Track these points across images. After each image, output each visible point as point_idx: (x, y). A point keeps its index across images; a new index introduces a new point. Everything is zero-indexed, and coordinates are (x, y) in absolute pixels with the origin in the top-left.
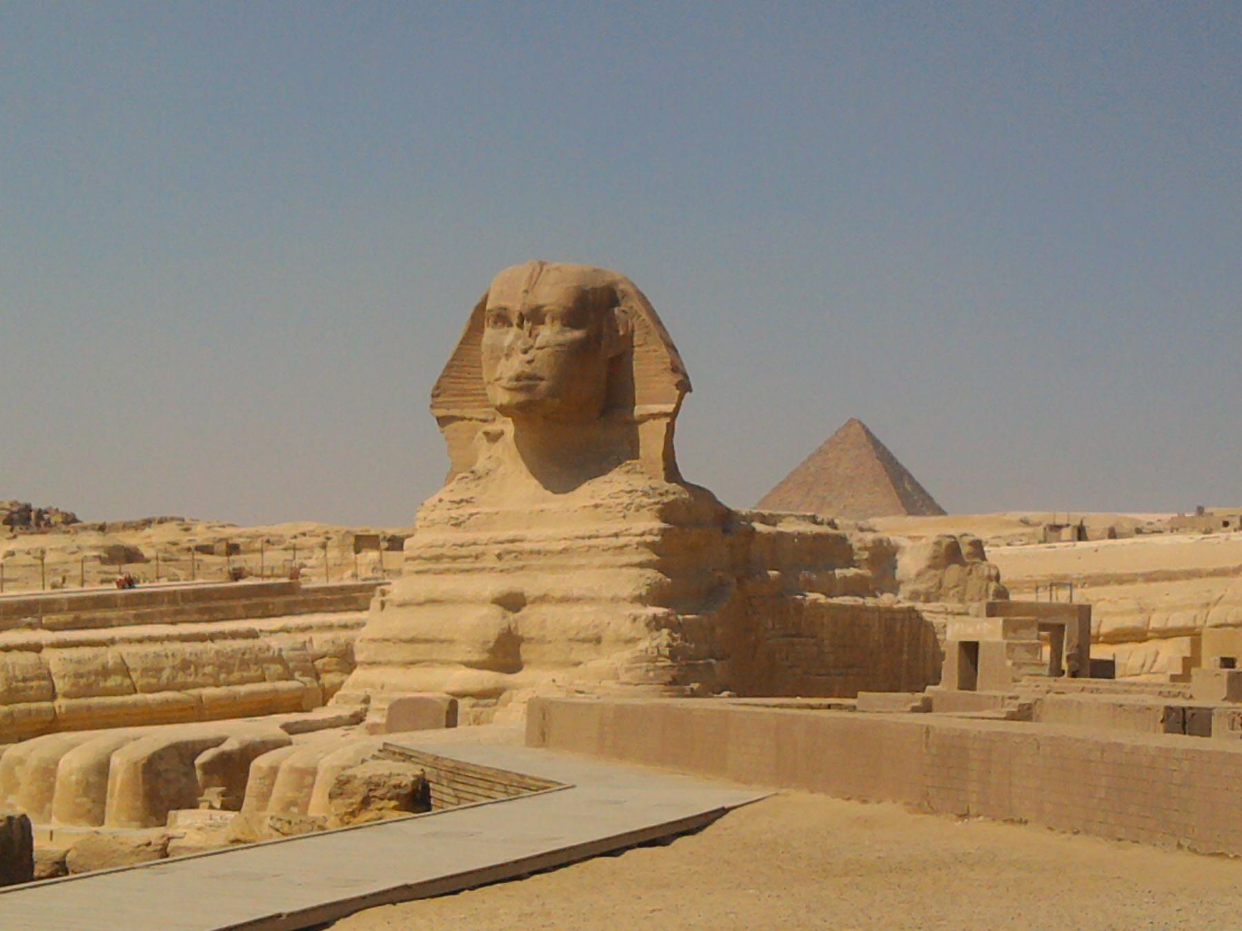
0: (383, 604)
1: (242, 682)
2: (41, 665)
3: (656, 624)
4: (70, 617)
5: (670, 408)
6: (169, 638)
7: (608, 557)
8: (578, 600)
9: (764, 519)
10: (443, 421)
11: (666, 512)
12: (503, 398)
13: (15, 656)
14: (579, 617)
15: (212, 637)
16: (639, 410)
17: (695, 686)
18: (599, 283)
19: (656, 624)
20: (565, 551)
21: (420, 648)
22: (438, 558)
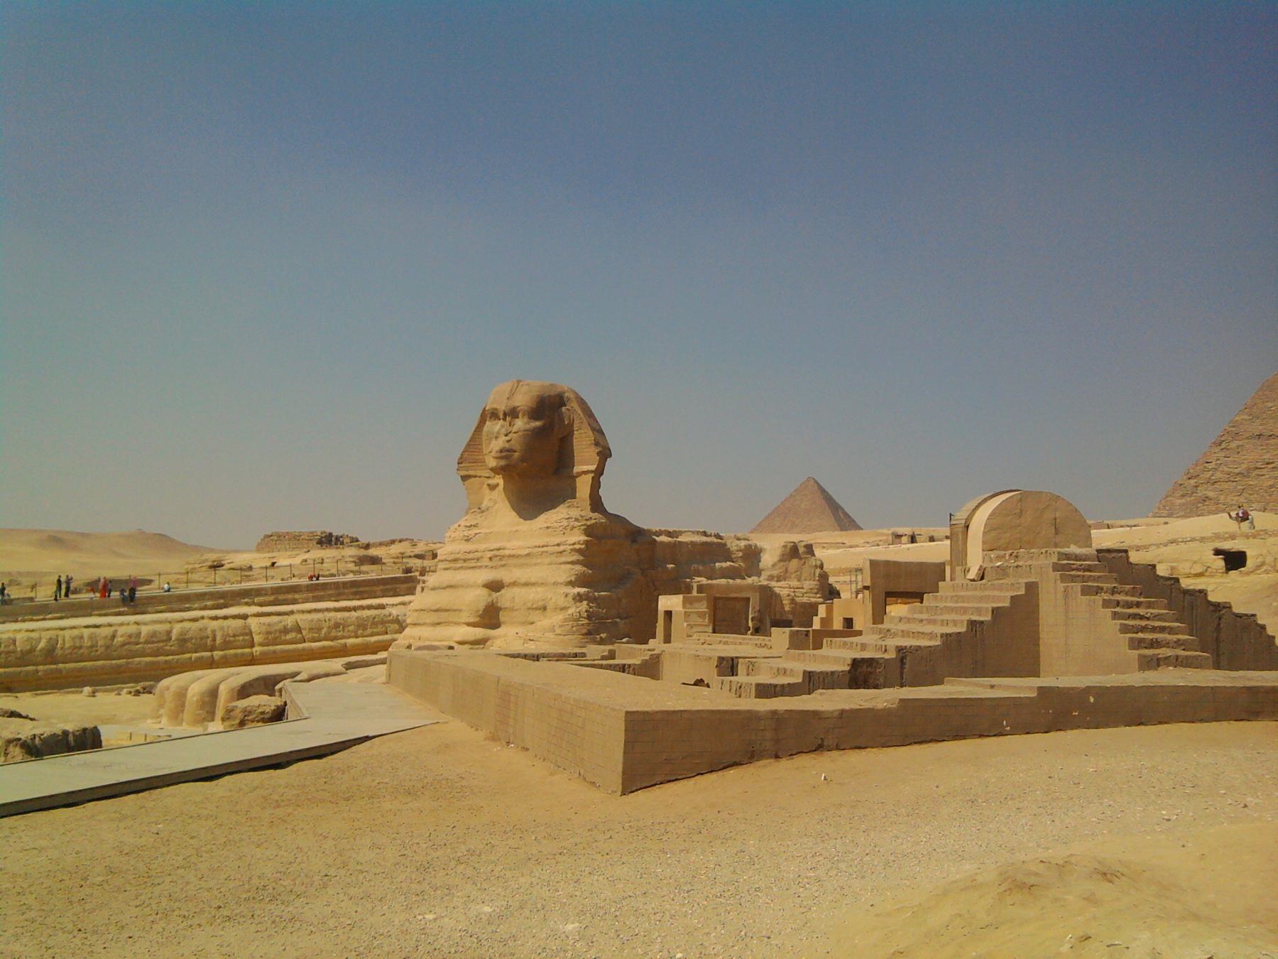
0: (423, 589)
3: (579, 598)
5: (593, 467)
7: (553, 558)
8: (534, 584)
11: (589, 531)
12: (492, 463)
14: (534, 595)
16: (577, 469)
17: (603, 635)
19: (579, 598)
20: (528, 555)
21: (442, 615)
22: (455, 560)
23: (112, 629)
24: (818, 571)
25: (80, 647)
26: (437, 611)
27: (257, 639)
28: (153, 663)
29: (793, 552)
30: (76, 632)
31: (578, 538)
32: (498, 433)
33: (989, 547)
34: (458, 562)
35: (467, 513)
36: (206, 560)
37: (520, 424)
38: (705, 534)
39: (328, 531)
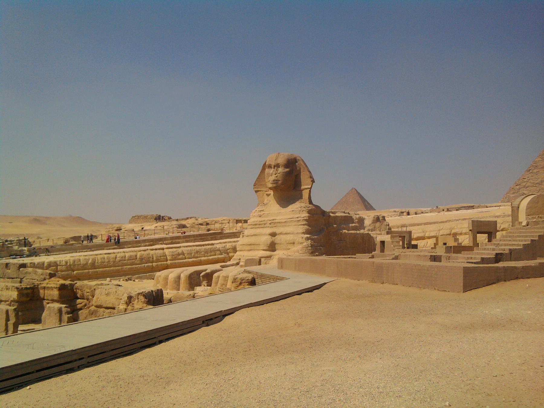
1: (211, 256)
2: (164, 253)
3: (307, 239)
4: (170, 241)
5: (310, 187)
6: (194, 246)
7: (296, 223)
8: (289, 233)
9: (333, 213)
10: (256, 192)
11: (309, 212)
13: (158, 251)
15: (203, 245)
16: (302, 187)
17: (317, 254)
18: (292, 158)
19: (307, 239)
21: (252, 246)
22: (256, 225)
23: (115, 255)
24: (387, 227)
25: (104, 262)
26: (250, 245)
27: (169, 258)
28: (131, 268)
29: (377, 219)
30: (102, 256)
31: (305, 215)
32: (272, 173)
33: (528, 215)
34: (255, 225)
35: (258, 206)
36: (114, 227)
37: (281, 170)
38: (344, 212)
39: (159, 214)
